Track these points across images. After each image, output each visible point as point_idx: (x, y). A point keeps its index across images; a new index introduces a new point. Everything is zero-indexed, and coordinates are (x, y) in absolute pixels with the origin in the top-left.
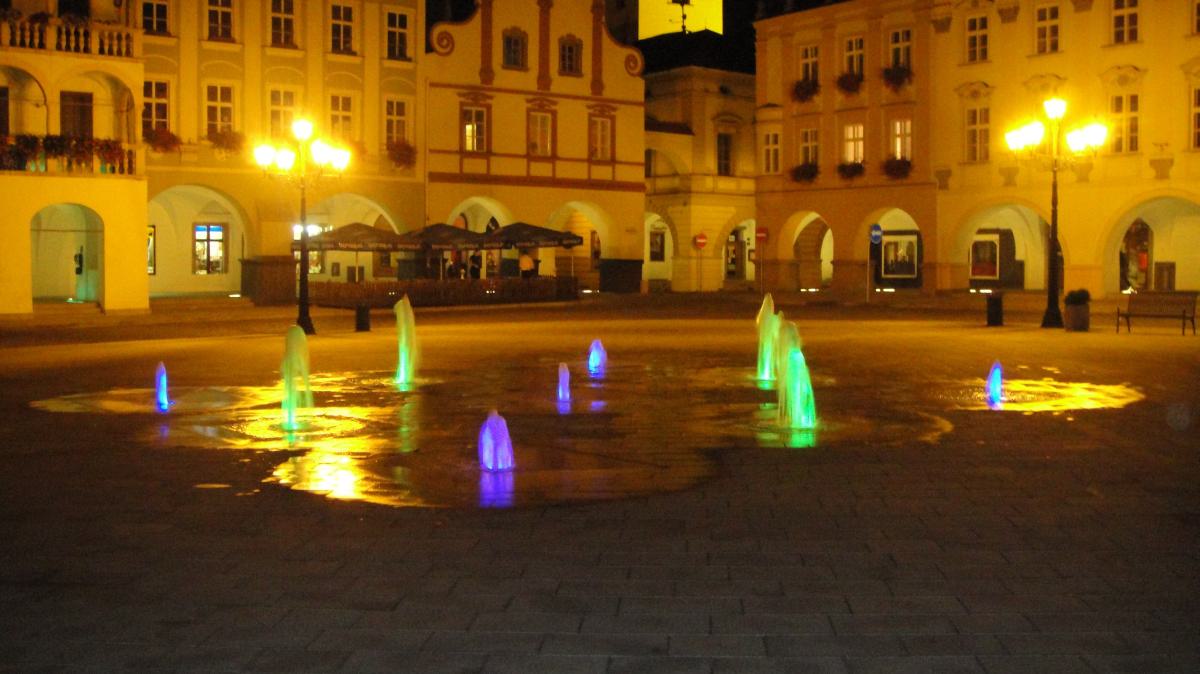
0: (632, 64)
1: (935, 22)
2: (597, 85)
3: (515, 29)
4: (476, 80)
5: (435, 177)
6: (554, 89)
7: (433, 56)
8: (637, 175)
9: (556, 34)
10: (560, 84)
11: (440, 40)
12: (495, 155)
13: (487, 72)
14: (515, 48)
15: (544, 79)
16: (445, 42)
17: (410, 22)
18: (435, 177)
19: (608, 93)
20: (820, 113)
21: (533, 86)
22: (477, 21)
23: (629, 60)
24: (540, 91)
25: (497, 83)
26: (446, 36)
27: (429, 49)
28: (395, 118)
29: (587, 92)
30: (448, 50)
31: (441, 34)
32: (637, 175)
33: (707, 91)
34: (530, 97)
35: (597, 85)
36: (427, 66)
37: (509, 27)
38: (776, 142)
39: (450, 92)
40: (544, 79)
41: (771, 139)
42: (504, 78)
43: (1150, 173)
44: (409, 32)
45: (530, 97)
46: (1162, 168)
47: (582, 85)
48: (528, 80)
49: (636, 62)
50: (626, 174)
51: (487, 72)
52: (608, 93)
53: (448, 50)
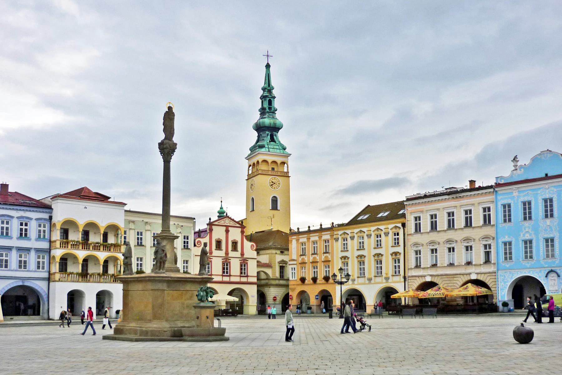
0: (253, 247)
1: (335, 239)
2: (242, 254)
3: (219, 239)
6: (230, 255)
7: (196, 247)
8: (255, 280)
9: (230, 239)
10: (232, 254)
11: (198, 243)
12: (213, 275)
14: (219, 243)
15: (227, 253)
16: (199, 244)
19: (245, 256)
20: (306, 263)
21: (224, 255)
23: (252, 246)
25: (213, 255)
27: (195, 245)
28: (185, 265)
29: (240, 256)
30: (200, 245)
31: (198, 241)
32: (255, 280)
33: (276, 253)
34: (223, 258)
35: (242, 254)
37: (217, 238)
38: (295, 270)
40: (227, 253)
41: (293, 269)
43: (384, 281)
44: (189, 240)
46: (387, 279)
48: (222, 253)
49: (254, 246)
50: (251, 280)
52: (245, 256)
53: (200, 245)
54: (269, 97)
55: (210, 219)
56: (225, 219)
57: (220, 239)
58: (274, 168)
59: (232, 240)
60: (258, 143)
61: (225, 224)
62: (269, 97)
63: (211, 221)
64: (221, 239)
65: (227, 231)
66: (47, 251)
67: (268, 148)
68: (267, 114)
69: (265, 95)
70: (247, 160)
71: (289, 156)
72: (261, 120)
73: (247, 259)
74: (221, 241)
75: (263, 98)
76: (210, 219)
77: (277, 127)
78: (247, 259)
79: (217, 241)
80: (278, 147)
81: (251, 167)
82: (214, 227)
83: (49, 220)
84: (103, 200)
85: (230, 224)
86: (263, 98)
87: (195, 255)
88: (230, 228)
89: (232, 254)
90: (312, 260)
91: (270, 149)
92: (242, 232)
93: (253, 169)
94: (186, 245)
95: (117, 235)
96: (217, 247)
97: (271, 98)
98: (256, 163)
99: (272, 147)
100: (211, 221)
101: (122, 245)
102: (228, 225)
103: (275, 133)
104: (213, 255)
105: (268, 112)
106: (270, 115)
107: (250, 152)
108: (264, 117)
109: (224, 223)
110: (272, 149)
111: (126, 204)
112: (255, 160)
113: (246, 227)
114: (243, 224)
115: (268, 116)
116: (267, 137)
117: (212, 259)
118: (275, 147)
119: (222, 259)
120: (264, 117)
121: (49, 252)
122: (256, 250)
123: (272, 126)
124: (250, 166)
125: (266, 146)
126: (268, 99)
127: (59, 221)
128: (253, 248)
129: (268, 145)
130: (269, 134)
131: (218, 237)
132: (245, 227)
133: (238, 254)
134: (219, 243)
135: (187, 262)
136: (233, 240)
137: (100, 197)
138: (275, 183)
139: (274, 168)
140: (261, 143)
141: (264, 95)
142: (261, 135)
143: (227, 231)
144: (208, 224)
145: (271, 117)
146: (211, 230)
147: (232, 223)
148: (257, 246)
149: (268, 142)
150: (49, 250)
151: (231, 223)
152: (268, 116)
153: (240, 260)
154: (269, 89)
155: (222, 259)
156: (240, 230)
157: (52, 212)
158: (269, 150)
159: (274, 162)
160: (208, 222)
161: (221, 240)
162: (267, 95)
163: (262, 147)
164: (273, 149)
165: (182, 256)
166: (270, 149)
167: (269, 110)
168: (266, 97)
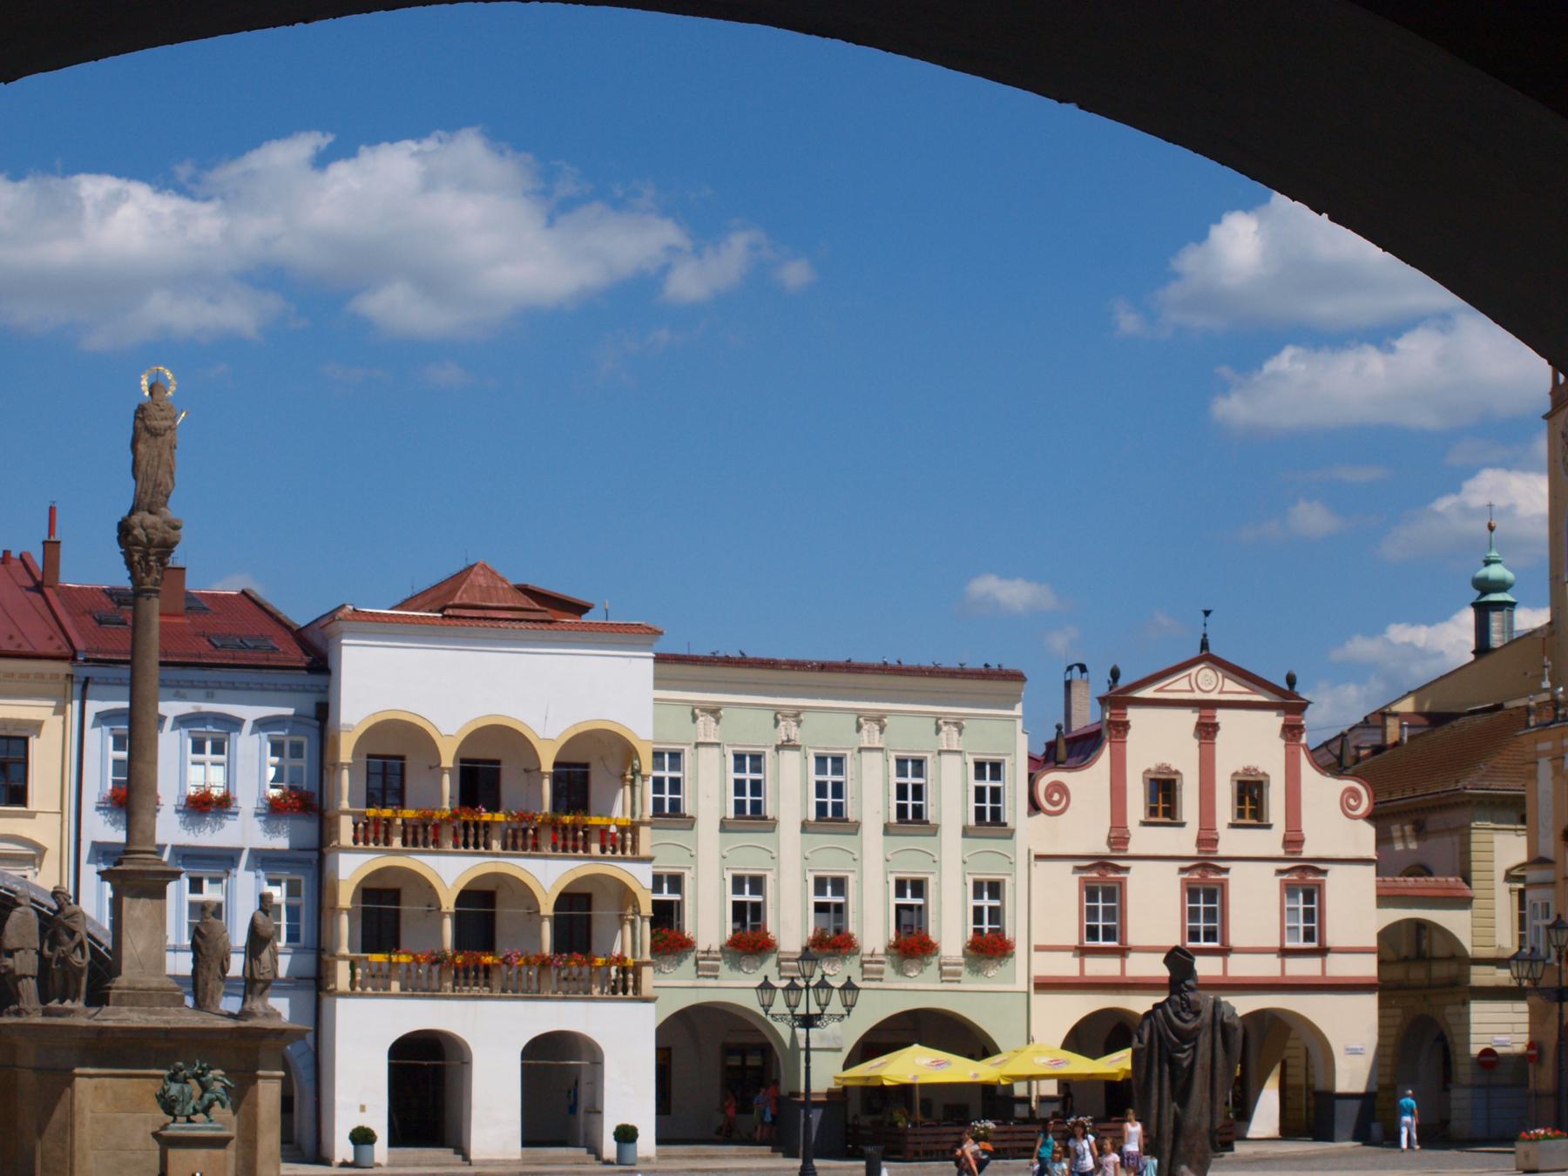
0: (1352, 802)
2: (1293, 841)
3: (1160, 769)
4: (1105, 850)
5: (1046, 985)
6: (1222, 850)
7: (1041, 818)
8: (1367, 967)
11: (1049, 797)
12: (1130, 949)
13: (1119, 838)
14: (1163, 792)
15: (1207, 840)
16: (1056, 797)
17: (1007, 770)
18: (1046, 985)
19: (1308, 851)
21: (1192, 851)
22: (1104, 761)
24: (1203, 855)
25: (1133, 849)
26: (1061, 788)
27: (1034, 807)
29: (1281, 852)
32: (1367, 967)
35: (1293, 841)
36: (1030, 832)
37: (1152, 766)
39: (1070, 865)
40: (1207, 840)
42: (1144, 839)
47: (1269, 841)
48: (1183, 841)
50: (1340, 967)
51: (1119, 838)
52: (1308, 851)
55: (1115, 674)
56: (1194, 671)
57: (1168, 768)
59: (1235, 774)
61: (1198, 695)
63: (1123, 682)
64: (1173, 768)
65: (1207, 731)
66: (310, 861)
73: (1321, 866)
74: (1174, 780)
76: (1115, 674)
78: (1321, 866)
79: (1152, 780)
82: (1133, 715)
83: (317, 723)
84: (550, 622)
85: (1221, 692)
87: (1039, 857)
88: (1222, 716)
89: (1231, 842)
92: (1291, 732)
95: (630, 777)
96: (1153, 811)
100: (1123, 682)
101: (643, 823)
102: (1214, 696)
104: (1133, 849)
109: (1192, 691)
111: (661, 633)
113: (1309, 703)
114: (1297, 688)
117: (1127, 869)
119: (1183, 870)
121: (315, 862)
122: (1371, 817)
127: (351, 728)
128: (1354, 809)
132: (1302, 707)
133: (1269, 841)
134: (1163, 792)
135: (995, 889)
137: (537, 607)
143: (1207, 731)
144: (1103, 701)
147: (1233, 689)
148: (1374, 795)
150: (315, 855)
151: (1230, 685)
153: (1280, 872)
155: (1183, 870)
157: (327, 687)
160: (1104, 690)
161: (1177, 772)
165: (964, 862)
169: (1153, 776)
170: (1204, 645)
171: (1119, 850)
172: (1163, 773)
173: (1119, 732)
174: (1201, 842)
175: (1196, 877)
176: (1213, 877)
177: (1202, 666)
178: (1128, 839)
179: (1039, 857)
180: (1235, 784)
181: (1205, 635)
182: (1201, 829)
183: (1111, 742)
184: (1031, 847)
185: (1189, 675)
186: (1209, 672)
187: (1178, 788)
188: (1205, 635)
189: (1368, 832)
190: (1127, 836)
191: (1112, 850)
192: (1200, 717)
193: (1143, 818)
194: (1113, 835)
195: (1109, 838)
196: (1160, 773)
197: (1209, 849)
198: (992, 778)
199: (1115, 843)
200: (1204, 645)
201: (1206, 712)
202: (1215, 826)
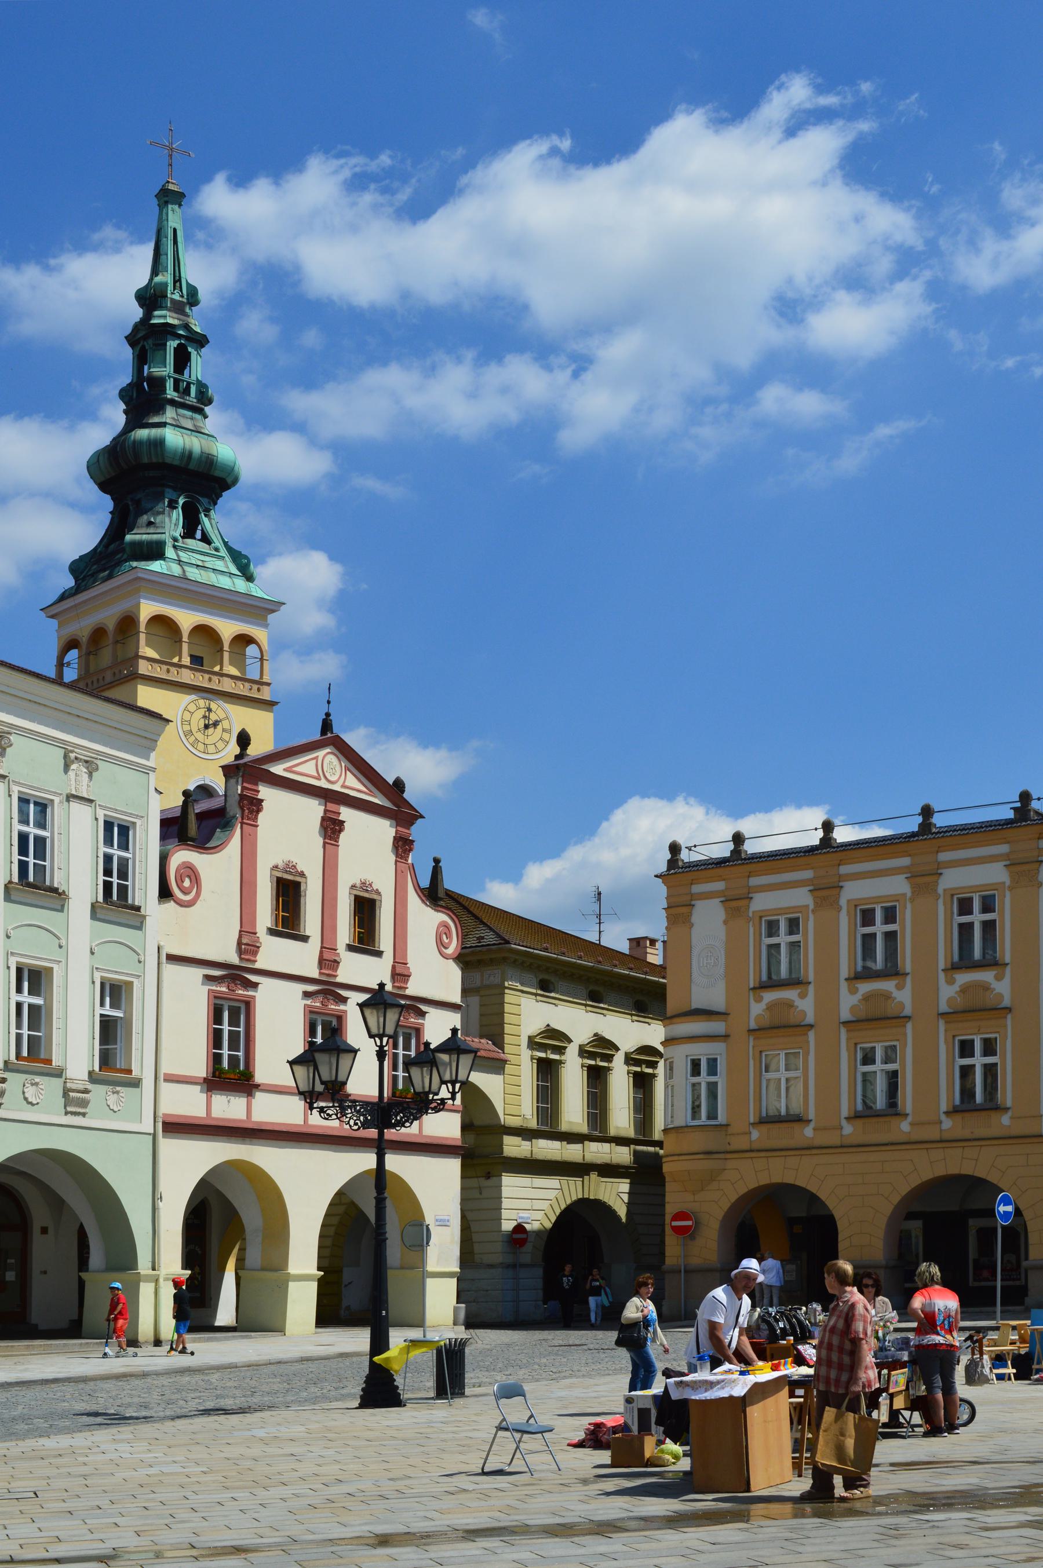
3: (290, 868)
4: (234, 959)
7: (171, 905)
11: (179, 880)
13: (247, 947)
15: (328, 961)
16: (187, 883)
24: (324, 978)
25: (262, 962)
27: (165, 893)
34: (311, 988)
39: (197, 973)
40: (328, 961)
45: (311, 988)
51: (247, 947)
54: (179, 337)
58: (202, 658)
59: (353, 887)
60: (128, 537)
62: (179, 337)
63: (254, 751)
64: (299, 869)
65: (332, 828)
67: (179, 562)
68: (170, 414)
69: (162, 321)
70: (54, 623)
71: (273, 611)
72: (142, 434)
74: (298, 884)
75: (145, 338)
77: (217, 474)
80: (219, 565)
81: (73, 655)
82: (265, 792)
85: (343, 786)
86: (145, 338)
87: (172, 958)
90: (853, 1009)
91: (187, 568)
92: (402, 846)
93: (91, 657)
94: (115, 880)
97: (186, 338)
98: (111, 625)
99: (196, 559)
100: (254, 751)
102: (336, 787)
103: (204, 501)
104: (262, 962)
105: (172, 402)
106: (184, 416)
107: (70, 582)
108: (156, 419)
109: (319, 779)
110: (195, 571)
112: (108, 616)
115: (173, 419)
116: (170, 517)
118: (210, 562)
120: (156, 419)
123: (191, 466)
124: (71, 644)
125: (170, 552)
126: (172, 344)
129: (175, 547)
130: (181, 501)
131: (286, 860)
136: (358, 884)
138: (206, 727)
139: (202, 658)
140: (144, 537)
141: (154, 321)
142: (138, 503)
143: (332, 828)
145: (190, 427)
146: (253, 806)
147: (352, 784)
148: (464, 936)
149: (177, 535)
152: (173, 419)
154: (177, 297)
155: (307, 995)
156: (384, 830)
158: (184, 571)
159: (203, 631)
161: (302, 874)
162: (170, 321)
163: (155, 551)
164: (202, 572)
166: (187, 568)
167: (176, 394)
168: (168, 330)
169: (280, 875)
170: (326, 726)
171: (248, 960)
172: (290, 873)
173: (251, 812)
174: (322, 962)
175: (318, 1004)
176: (333, 1007)
177: (328, 750)
178: (259, 947)
179: (172, 958)
180: (353, 898)
181: (328, 715)
182: (322, 947)
183: (242, 823)
184: (162, 944)
185: (316, 758)
186: (332, 758)
187: (303, 894)
188: (328, 715)
189: (454, 974)
190: (258, 945)
191: (241, 959)
192: (326, 811)
193: (269, 926)
194: (244, 941)
195: (239, 943)
196: (286, 872)
197: (331, 972)
198: (120, 847)
199: (246, 952)
200: (326, 726)
201: (331, 806)
202: (336, 945)
